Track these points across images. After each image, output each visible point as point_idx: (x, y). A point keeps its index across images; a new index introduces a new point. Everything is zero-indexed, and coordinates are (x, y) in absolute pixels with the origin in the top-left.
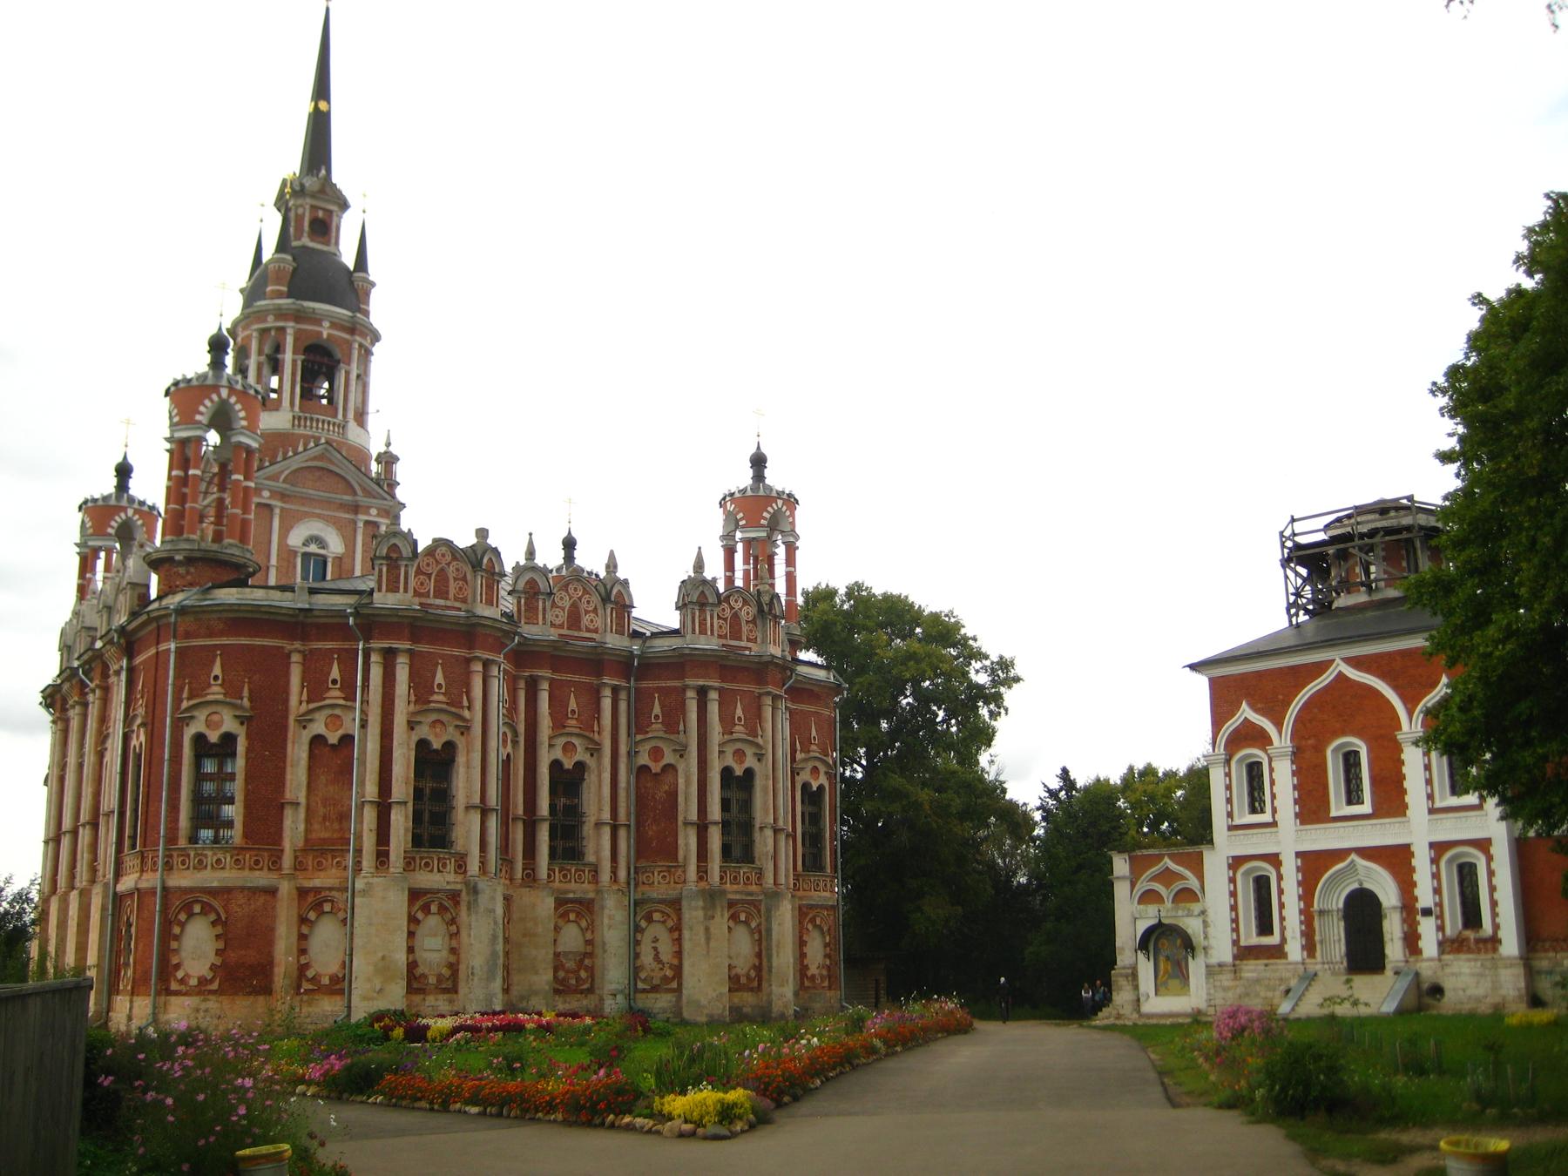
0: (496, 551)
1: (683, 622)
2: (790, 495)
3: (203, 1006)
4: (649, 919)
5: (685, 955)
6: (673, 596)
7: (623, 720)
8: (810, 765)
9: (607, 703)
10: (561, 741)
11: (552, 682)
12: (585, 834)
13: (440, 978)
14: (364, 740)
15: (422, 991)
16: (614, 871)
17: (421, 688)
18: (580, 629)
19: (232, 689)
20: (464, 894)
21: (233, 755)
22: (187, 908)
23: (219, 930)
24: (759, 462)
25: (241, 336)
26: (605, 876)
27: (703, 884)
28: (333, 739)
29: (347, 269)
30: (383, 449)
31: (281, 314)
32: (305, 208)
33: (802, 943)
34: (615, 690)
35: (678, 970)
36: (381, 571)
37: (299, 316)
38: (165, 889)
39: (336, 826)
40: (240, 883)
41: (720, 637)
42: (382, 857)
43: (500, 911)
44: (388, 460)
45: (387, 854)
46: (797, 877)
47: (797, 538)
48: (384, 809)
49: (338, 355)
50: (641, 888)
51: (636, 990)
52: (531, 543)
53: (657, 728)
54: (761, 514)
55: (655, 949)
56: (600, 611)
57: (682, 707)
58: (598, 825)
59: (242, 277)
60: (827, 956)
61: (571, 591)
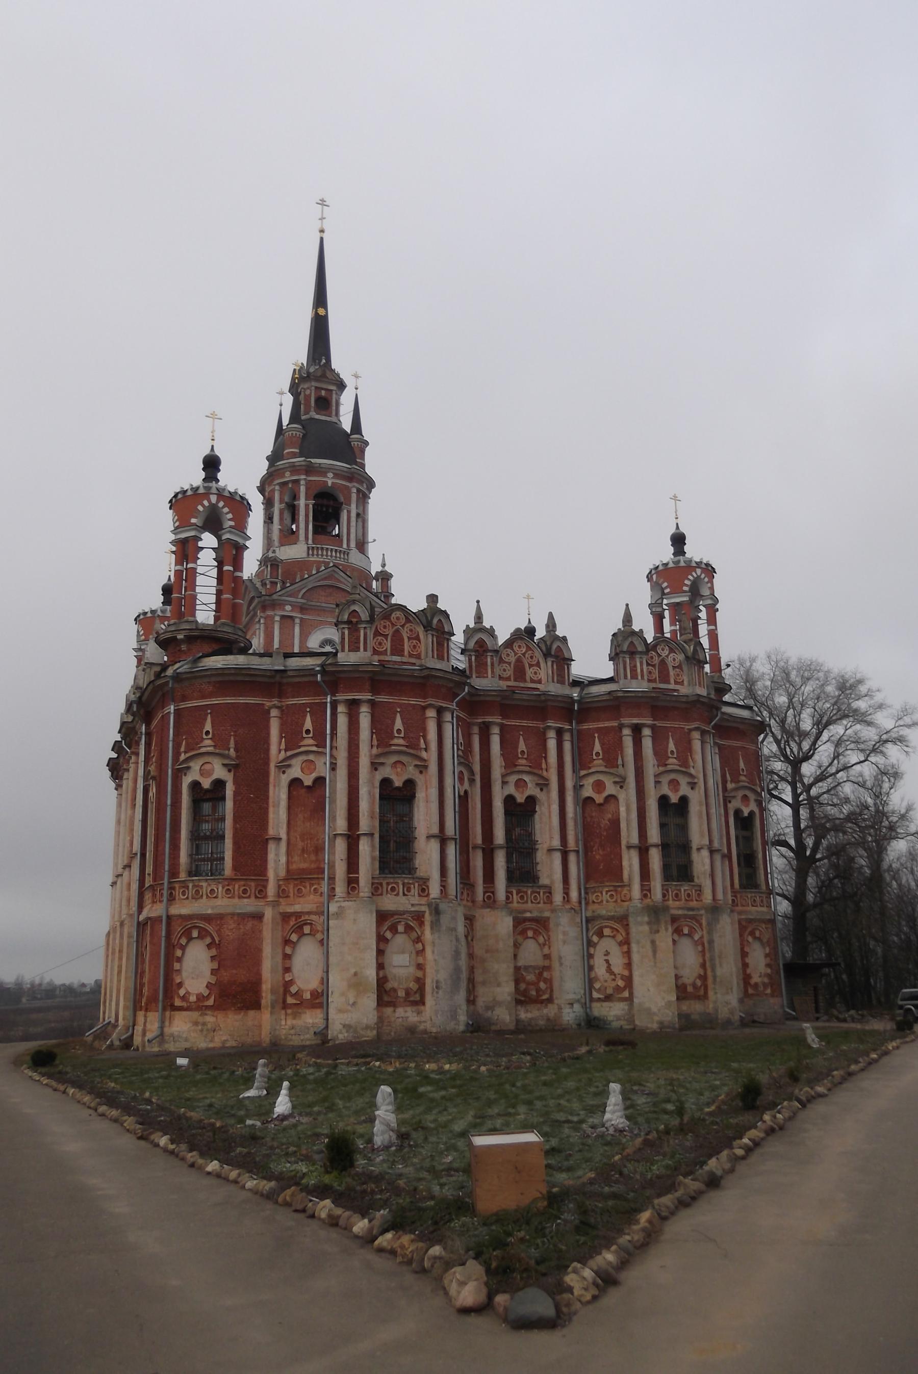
0: (445, 614)
1: (616, 670)
2: (707, 565)
3: (201, 1020)
4: (600, 934)
5: (635, 967)
6: (606, 648)
7: (568, 758)
8: (740, 794)
9: (552, 744)
10: (513, 779)
11: (502, 727)
12: (538, 860)
13: (408, 992)
14: (333, 781)
15: (393, 1004)
16: (566, 892)
17: (381, 731)
18: (525, 681)
19: (220, 741)
20: (427, 915)
21: (223, 798)
22: (187, 933)
23: (214, 952)
24: (679, 541)
25: (268, 489)
26: (558, 898)
27: (648, 901)
28: (308, 781)
30: (380, 569)
31: (294, 469)
32: (309, 390)
33: (744, 954)
34: (560, 733)
35: (629, 980)
36: (343, 634)
37: (310, 470)
38: (169, 917)
39: (313, 857)
40: (230, 910)
41: (649, 681)
42: (352, 883)
43: (461, 929)
44: (385, 577)
45: (356, 881)
46: (734, 893)
47: (716, 601)
48: (352, 840)
49: (342, 499)
50: (592, 907)
51: (592, 1000)
52: (479, 608)
53: (598, 764)
54: (684, 584)
55: (607, 961)
56: (542, 665)
57: (619, 745)
58: (550, 850)
59: (268, 448)
60: (768, 965)
61: (516, 648)
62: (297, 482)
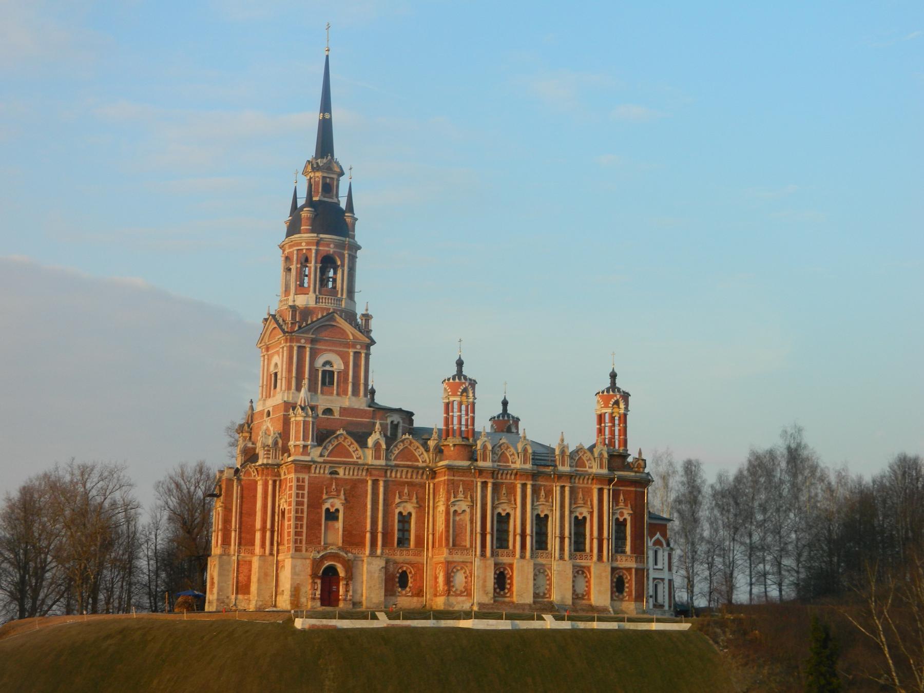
29: (341, 209)
44: (367, 317)
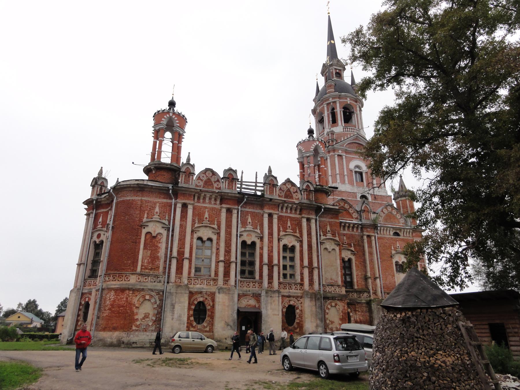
37: (340, 97)
62: (335, 102)
